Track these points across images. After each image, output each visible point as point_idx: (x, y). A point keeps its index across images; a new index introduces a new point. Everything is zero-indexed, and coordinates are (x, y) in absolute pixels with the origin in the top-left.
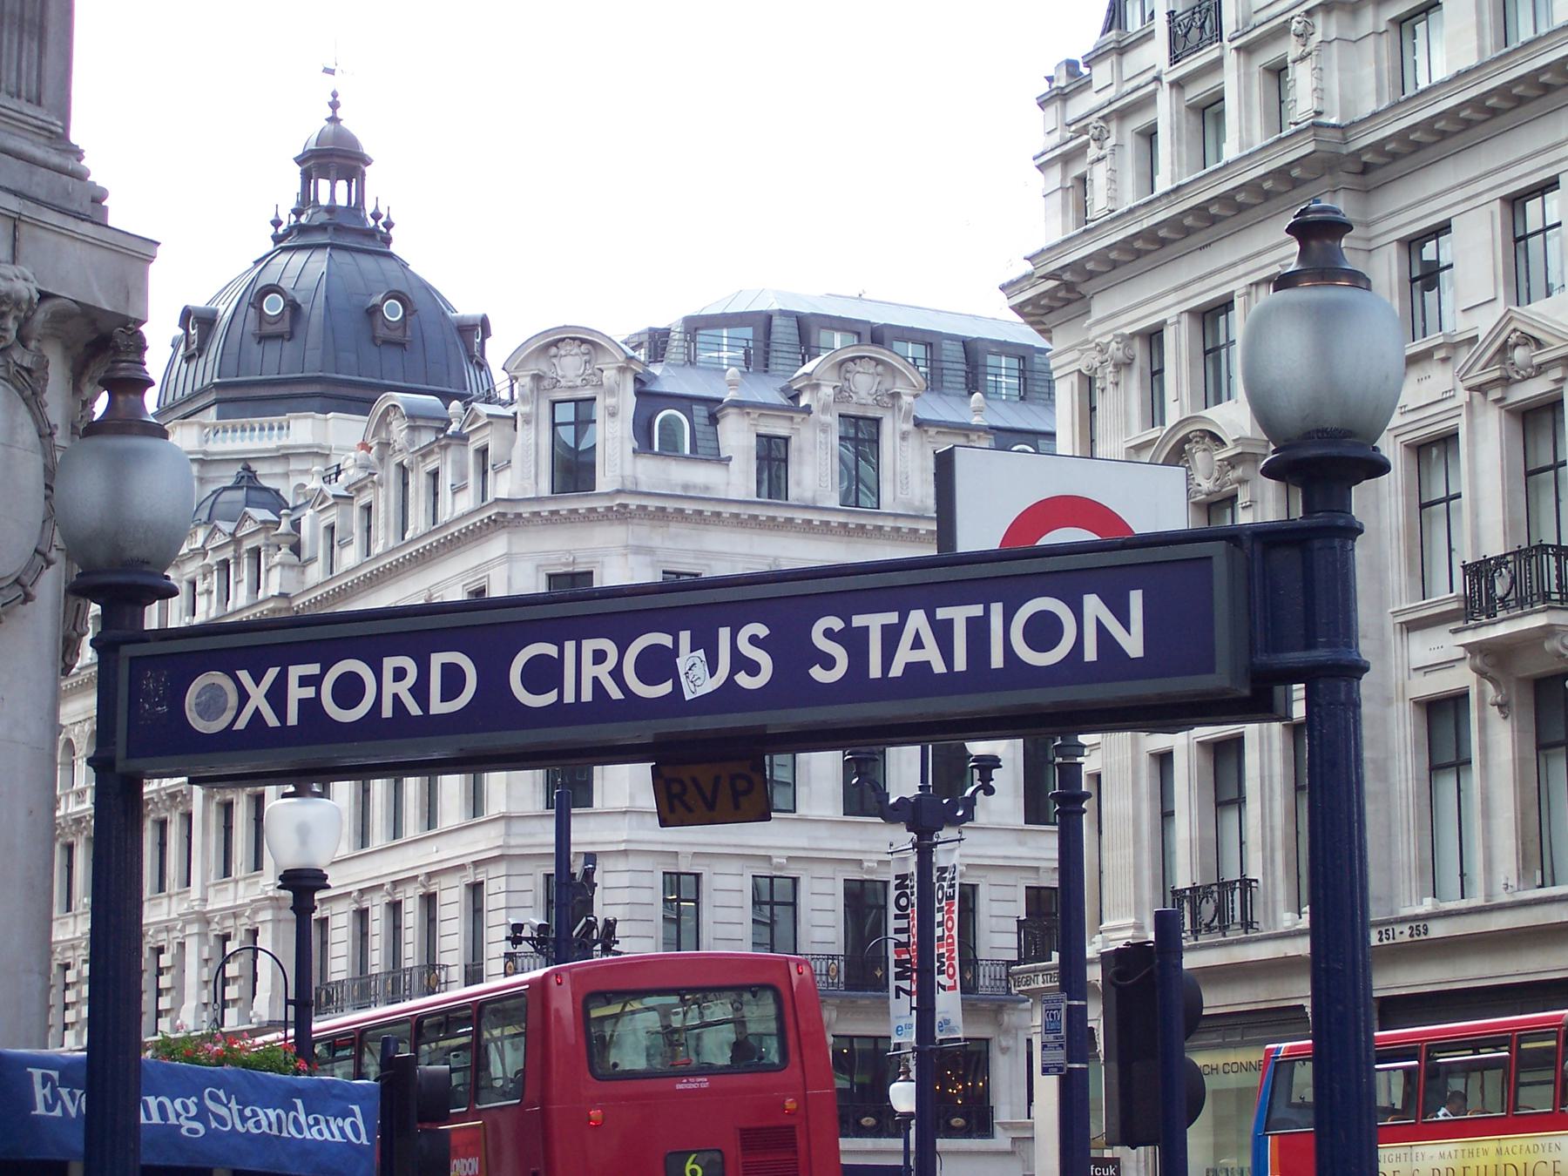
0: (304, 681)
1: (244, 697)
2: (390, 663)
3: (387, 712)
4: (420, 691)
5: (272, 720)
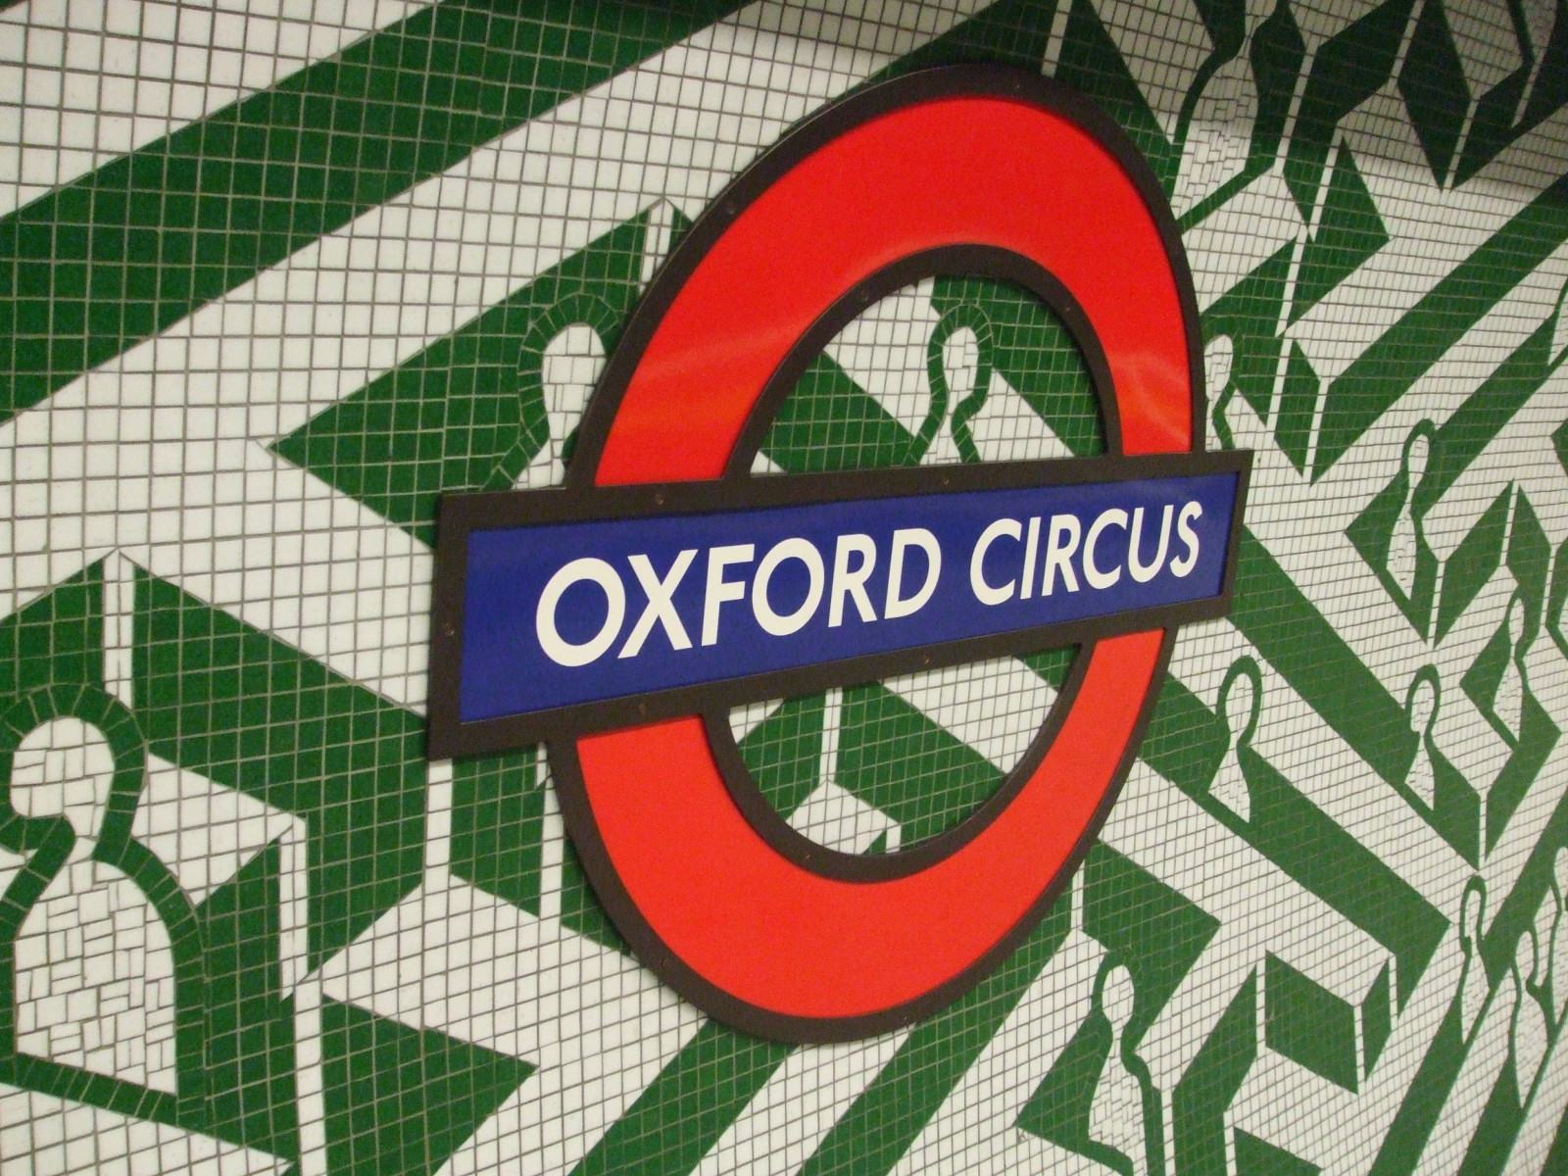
0: (732, 573)
1: (637, 600)
2: (846, 544)
3: (835, 619)
4: (876, 588)
5: (680, 640)
